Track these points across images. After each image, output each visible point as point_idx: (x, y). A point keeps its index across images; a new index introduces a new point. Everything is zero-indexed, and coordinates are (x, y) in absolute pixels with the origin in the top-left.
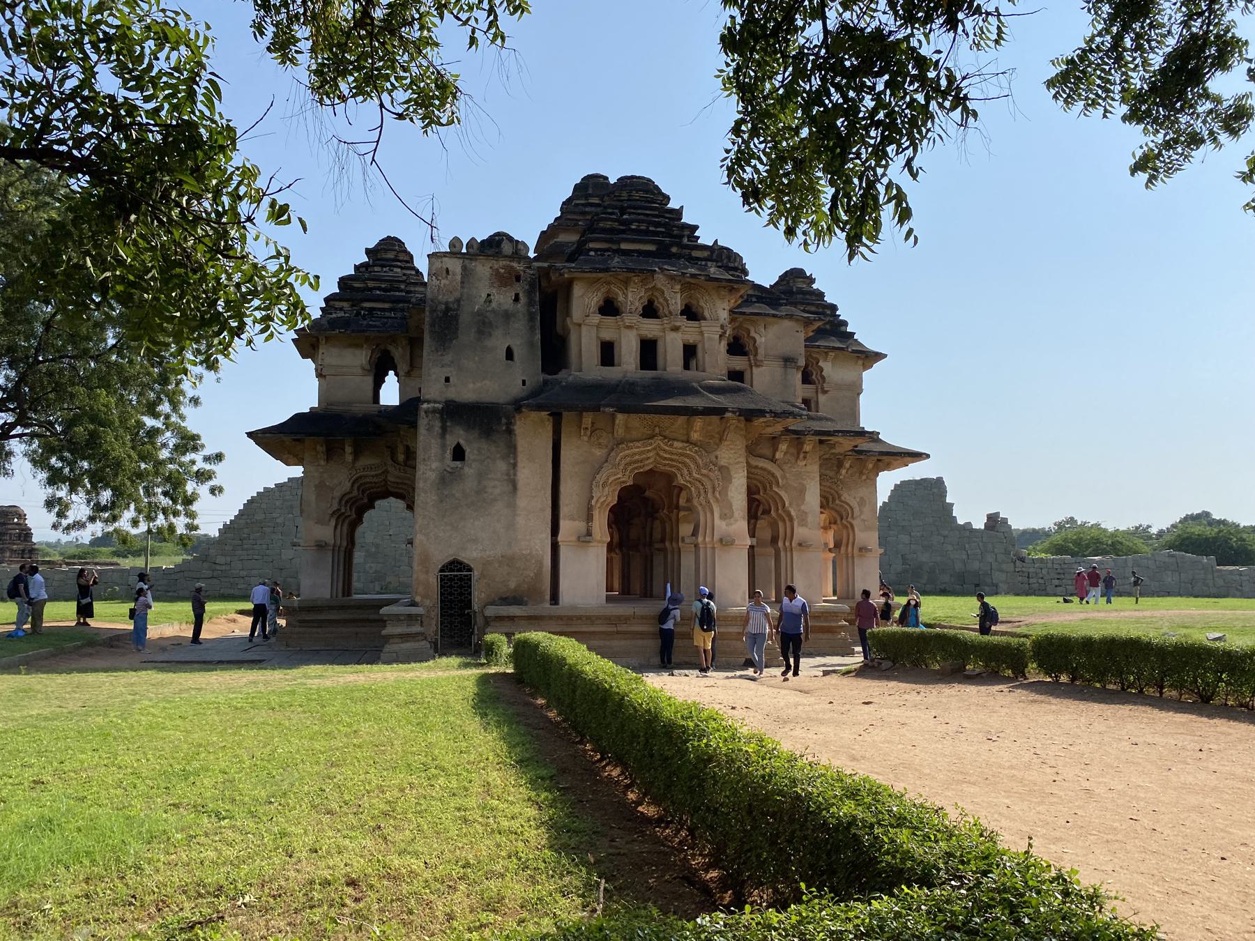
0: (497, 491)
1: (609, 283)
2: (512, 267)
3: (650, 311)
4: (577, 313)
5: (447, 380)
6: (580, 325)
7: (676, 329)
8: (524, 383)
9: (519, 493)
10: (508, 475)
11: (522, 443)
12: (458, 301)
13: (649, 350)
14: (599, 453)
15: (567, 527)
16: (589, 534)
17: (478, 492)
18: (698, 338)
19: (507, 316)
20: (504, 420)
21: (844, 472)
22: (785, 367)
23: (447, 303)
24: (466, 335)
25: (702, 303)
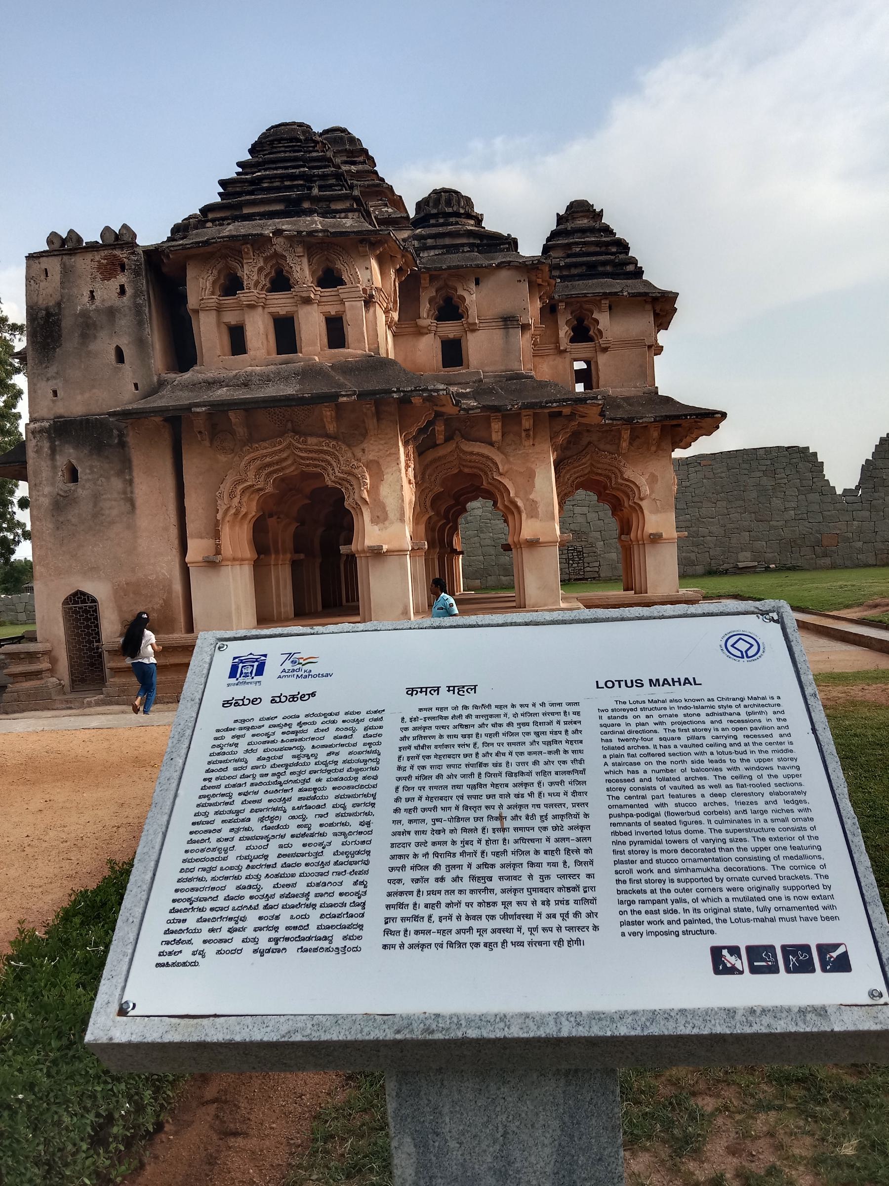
0: (115, 512)
1: (225, 257)
2: (115, 256)
3: (281, 282)
4: (192, 302)
5: (55, 393)
6: (197, 312)
7: (307, 301)
8: (136, 385)
9: (138, 511)
10: (125, 493)
11: (137, 458)
12: (59, 304)
13: (285, 334)
14: (223, 458)
15: (197, 548)
16: (218, 552)
17: (95, 516)
18: (339, 308)
19: (111, 313)
20: (115, 432)
21: (624, 445)
22: (506, 327)
23: (47, 309)
24: (70, 343)
25: (339, 265)
